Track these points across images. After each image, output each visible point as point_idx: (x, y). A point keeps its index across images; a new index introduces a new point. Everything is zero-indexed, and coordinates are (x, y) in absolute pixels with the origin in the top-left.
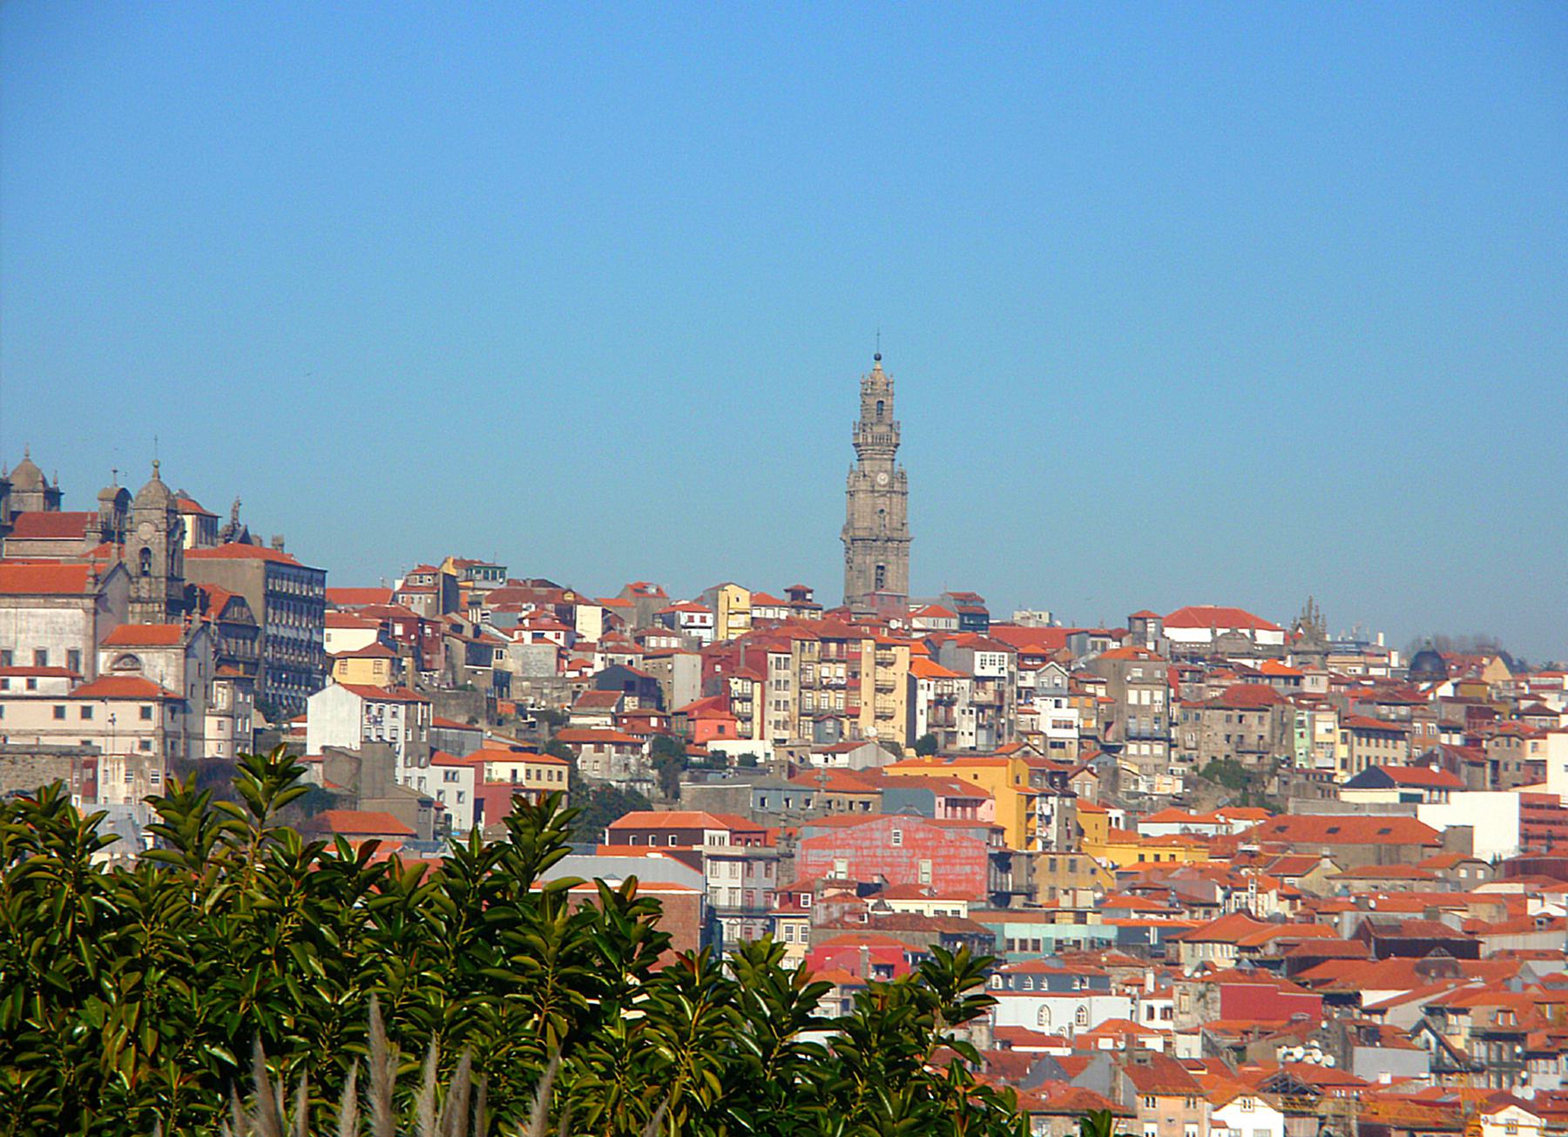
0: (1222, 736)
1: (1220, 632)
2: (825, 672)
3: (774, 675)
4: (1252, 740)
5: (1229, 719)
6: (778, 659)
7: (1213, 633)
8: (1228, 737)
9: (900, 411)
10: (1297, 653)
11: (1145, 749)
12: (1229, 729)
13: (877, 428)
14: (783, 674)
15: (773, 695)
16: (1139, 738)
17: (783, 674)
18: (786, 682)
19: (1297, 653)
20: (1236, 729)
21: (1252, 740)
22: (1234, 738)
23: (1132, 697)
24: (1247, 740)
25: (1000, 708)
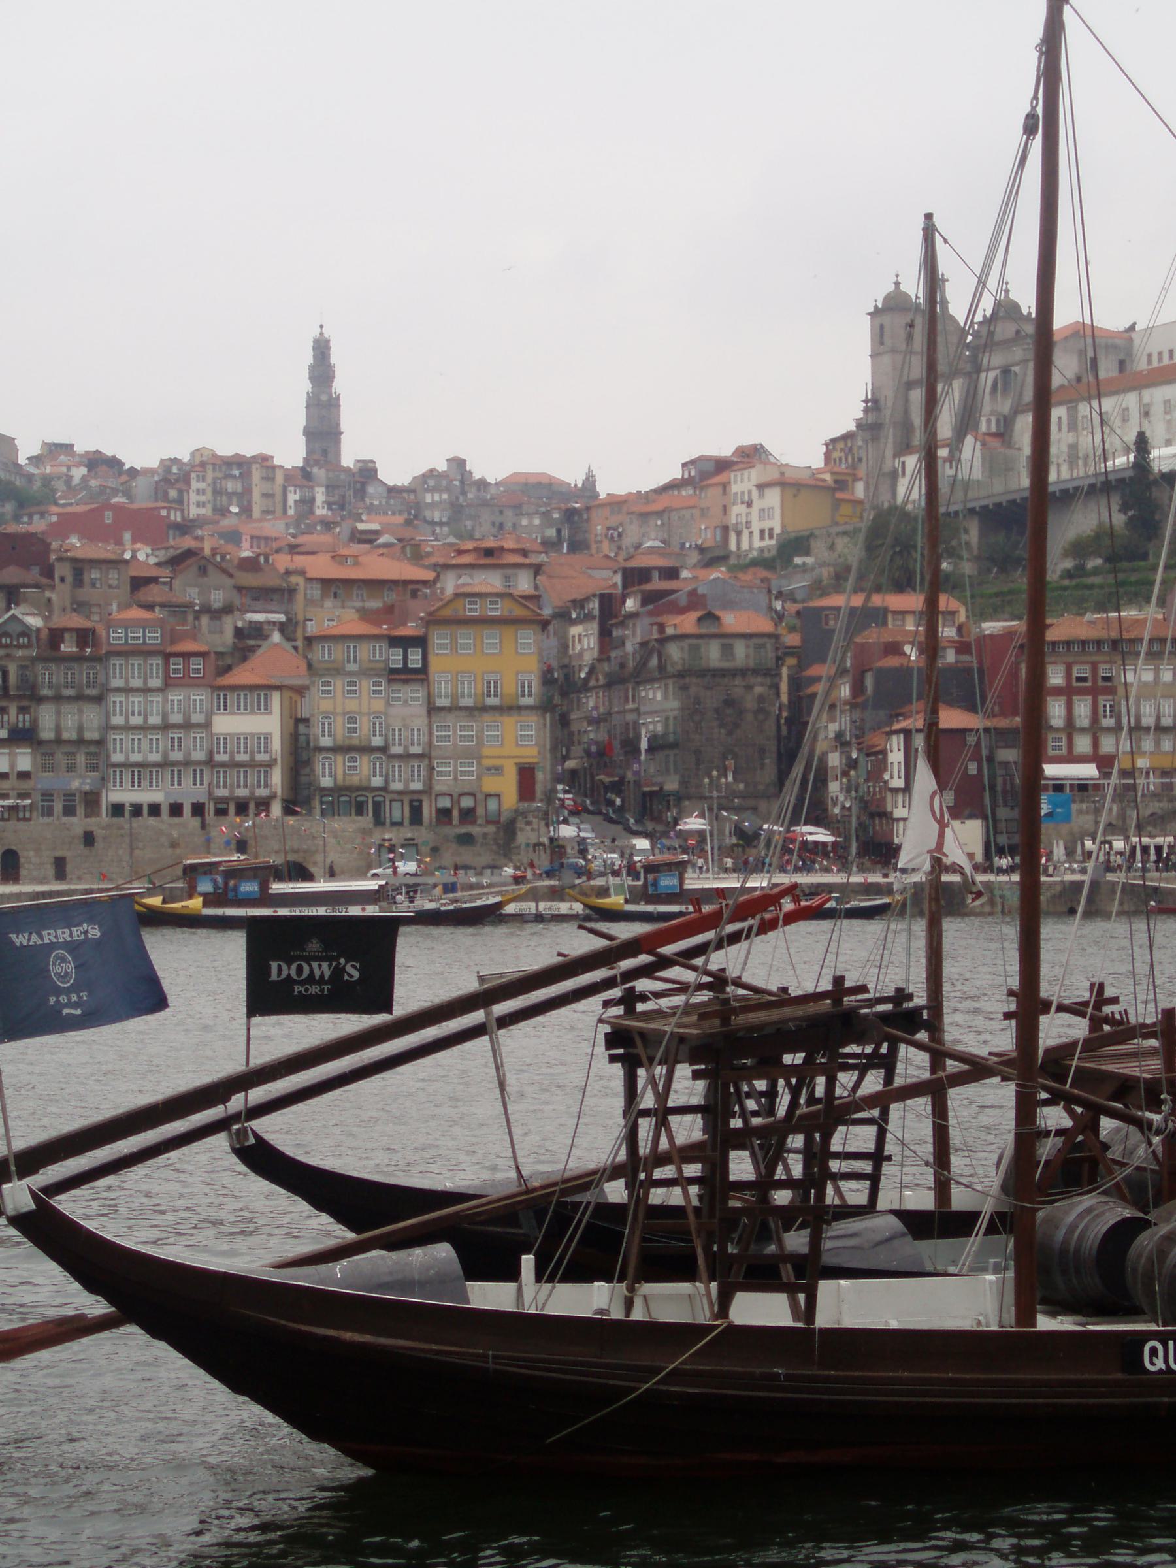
3: (195, 485)
8: (493, 524)
9: (335, 358)
13: (322, 370)
14: (202, 485)
15: (194, 498)
17: (202, 485)
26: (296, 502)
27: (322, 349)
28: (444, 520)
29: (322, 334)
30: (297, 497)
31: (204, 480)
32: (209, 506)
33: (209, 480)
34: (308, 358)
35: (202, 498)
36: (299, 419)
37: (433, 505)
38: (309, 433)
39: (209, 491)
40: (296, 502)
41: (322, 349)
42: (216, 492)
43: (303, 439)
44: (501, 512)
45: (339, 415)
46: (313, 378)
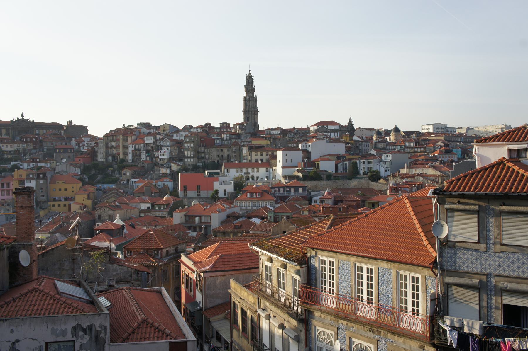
0: (216, 155)
2: (113, 144)
4: (225, 156)
5: (218, 151)
8: (218, 156)
11: (189, 160)
12: (218, 153)
16: (187, 157)
22: (220, 156)
23: (185, 145)
24: (224, 156)
26: (132, 151)
27: (250, 80)
28: (192, 156)
29: (250, 74)
30: (133, 149)
32: (104, 154)
34: (245, 83)
37: (187, 149)
38: (246, 112)
40: (132, 151)
41: (250, 80)
43: (243, 113)
44: (222, 150)
46: (247, 90)
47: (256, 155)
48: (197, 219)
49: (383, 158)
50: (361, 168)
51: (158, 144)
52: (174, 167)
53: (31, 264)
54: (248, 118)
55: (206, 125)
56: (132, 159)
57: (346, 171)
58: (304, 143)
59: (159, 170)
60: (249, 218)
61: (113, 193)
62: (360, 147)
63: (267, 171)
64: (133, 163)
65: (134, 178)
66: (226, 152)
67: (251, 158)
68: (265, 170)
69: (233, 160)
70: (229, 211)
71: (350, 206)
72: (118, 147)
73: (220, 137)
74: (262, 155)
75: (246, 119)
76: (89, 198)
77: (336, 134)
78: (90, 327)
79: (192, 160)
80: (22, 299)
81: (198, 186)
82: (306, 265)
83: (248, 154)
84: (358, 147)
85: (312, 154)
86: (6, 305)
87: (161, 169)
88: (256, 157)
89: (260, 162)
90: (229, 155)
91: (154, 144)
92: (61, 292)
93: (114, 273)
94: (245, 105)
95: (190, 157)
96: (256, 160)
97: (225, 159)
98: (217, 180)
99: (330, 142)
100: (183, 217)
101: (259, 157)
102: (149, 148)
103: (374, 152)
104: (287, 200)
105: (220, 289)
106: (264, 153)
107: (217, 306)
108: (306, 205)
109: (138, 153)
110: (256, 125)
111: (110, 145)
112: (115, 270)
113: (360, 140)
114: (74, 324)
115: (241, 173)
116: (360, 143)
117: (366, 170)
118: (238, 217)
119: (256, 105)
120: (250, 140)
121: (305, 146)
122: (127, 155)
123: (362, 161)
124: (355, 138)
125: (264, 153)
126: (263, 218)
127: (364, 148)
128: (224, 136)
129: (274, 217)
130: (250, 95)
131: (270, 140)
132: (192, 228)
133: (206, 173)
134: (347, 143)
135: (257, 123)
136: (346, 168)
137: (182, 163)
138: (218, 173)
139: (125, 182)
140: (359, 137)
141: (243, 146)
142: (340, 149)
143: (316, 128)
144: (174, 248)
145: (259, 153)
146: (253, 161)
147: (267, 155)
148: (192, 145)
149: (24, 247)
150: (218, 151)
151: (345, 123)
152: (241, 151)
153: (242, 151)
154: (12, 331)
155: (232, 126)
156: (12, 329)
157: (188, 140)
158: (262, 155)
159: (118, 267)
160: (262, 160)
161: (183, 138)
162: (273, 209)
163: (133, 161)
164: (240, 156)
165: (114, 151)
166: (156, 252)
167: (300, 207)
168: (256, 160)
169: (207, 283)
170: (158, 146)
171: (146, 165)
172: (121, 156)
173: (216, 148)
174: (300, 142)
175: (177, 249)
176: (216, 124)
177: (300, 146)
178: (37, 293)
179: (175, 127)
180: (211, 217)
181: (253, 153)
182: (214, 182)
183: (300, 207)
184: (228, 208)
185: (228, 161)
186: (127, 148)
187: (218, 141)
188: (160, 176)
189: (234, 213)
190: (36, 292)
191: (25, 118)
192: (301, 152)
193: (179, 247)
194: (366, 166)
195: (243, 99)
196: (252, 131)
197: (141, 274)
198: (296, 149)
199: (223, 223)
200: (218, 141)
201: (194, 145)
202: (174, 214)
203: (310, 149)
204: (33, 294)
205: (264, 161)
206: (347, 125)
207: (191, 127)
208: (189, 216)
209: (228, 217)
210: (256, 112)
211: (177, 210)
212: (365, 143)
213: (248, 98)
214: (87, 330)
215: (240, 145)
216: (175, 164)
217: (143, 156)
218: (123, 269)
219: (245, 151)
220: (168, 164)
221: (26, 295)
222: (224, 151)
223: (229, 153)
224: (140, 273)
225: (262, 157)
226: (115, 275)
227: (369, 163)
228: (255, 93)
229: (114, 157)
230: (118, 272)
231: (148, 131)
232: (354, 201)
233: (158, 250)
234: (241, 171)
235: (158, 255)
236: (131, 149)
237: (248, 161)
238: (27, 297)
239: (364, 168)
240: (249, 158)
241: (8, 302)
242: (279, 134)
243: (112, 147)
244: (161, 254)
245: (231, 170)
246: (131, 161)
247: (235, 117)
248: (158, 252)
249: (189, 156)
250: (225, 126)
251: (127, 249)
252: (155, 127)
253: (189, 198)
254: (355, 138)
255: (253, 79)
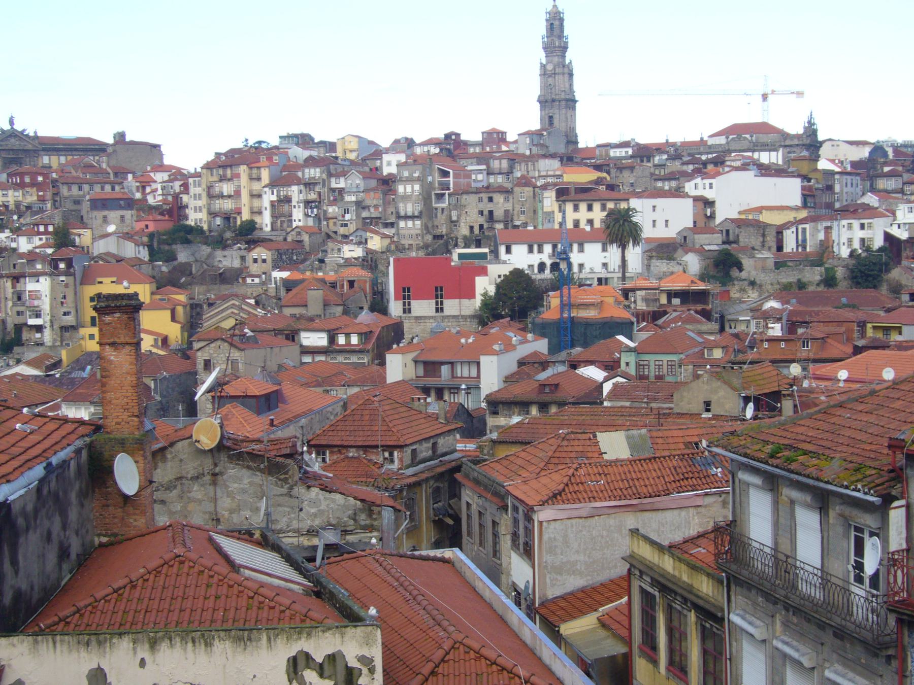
0: (476, 211)
1: (731, 137)
5: (480, 200)
6: (195, 181)
7: (727, 138)
10: (785, 146)
11: (410, 224)
12: (481, 206)
14: (198, 190)
16: (406, 217)
17: (198, 190)
18: (200, 195)
19: (785, 146)
20: (487, 207)
21: (499, 213)
24: (495, 214)
25: (320, 202)
26: (272, 203)
29: (555, 6)
31: (200, 185)
32: (205, 211)
33: (204, 186)
34: (542, 29)
35: (199, 203)
36: (534, 88)
37: (406, 198)
38: (545, 102)
39: (204, 195)
42: (211, 196)
43: (538, 105)
44: (491, 199)
45: (541, 82)
46: (549, 49)
47: (576, 208)
48: (445, 370)
49: (899, 214)
50: (844, 239)
51: (334, 185)
52: (375, 243)
53: (141, 489)
54: (551, 118)
55: (448, 136)
56: (272, 224)
57: (804, 247)
58: (698, 180)
59: (339, 250)
60: (574, 366)
61: (233, 306)
62: (837, 188)
63: (604, 250)
64: (274, 233)
65: (277, 266)
66: (500, 204)
67: (564, 218)
68: (599, 246)
69: (517, 223)
70: (524, 351)
71: (829, 335)
72: (238, 193)
73: (484, 167)
74: (590, 208)
75: (549, 121)
76: (173, 319)
77: (773, 154)
78: (332, 658)
79: (418, 223)
80: (150, 582)
81: (436, 288)
82: (903, 502)
83: (556, 209)
84: (830, 188)
85: (717, 205)
86: (115, 595)
87: (346, 248)
88: (576, 216)
89: (588, 228)
90: (506, 212)
91: (324, 185)
92: (241, 566)
93: (313, 511)
94: (545, 86)
95: (413, 217)
96: (577, 223)
97: (499, 221)
98: (483, 272)
99: (763, 175)
100: (411, 365)
101: (583, 214)
102: (313, 196)
103: (871, 199)
104: (660, 322)
105: (577, 552)
106: (597, 206)
107: (572, 594)
108: (711, 333)
109: (286, 208)
110: (571, 139)
111: (217, 189)
112: (314, 503)
113: (837, 169)
114: (293, 649)
115: (541, 256)
116: (837, 177)
117: (856, 245)
118: (544, 365)
119: (571, 85)
120: (558, 173)
121: (700, 186)
122: (260, 213)
123: (844, 222)
124: (823, 164)
125: (597, 206)
126: (611, 367)
127: (845, 190)
128: (495, 164)
129: (638, 366)
130: (556, 59)
131: (608, 173)
132: (433, 394)
133: (455, 257)
134: (805, 178)
135: (573, 129)
136: (804, 241)
137: (393, 231)
138: (483, 256)
139: (257, 280)
140: (833, 161)
141: (544, 187)
142: (789, 191)
143: (722, 140)
144: (430, 445)
145: (583, 206)
146: (570, 225)
147: (603, 208)
148: (417, 187)
149: (123, 445)
150: (480, 200)
151: (795, 127)
152: (536, 198)
153: (541, 201)
154: (143, 663)
155: (511, 137)
156: (143, 660)
157: (406, 174)
158: (590, 208)
159: (322, 495)
160: (590, 222)
161: (393, 170)
162: (632, 344)
163: (273, 229)
164: (535, 212)
165: (227, 205)
166: (387, 454)
167: (700, 340)
168: (577, 223)
169: (545, 537)
170: (333, 190)
171: (306, 238)
172: (246, 216)
173: (476, 193)
174: (690, 176)
175: (434, 445)
176: (472, 134)
177: (689, 187)
178: (185, 569)
179: (371, 143)
180: (478, 364)
181: (569, 207)
182: (477, 279)
183: (700, 340)
184: (521, 343)
185: (506, 227)
186: (260, 196)
187: (480, 177)
188: (340, 266)
189: (536, 354)
190: (182, 563)
191: (18, 127)
192: (690, 201)
193: (441, 441)
194: (859, 234)
195: (537, 71)
196: (561, 149)
197: (379, 513)
198: (678, 193)
199: (508, 379)
200: (480, 177)
201: (422, 186)
202: (389, 358)
203: (709, 194)
204: (175, 569)
205: (597, 224)
206: (801, 131)
207: (410, 143)
208: (426, 363)
209: (521, 363)
210: (571, 103)
211: (395, 346)
212: (849, 178)
213: (550, 67)
214: (326, 666)
215: (535, 187)
216: (377, 233)
217: (298, 215)
218: (334, 501)
219: (549, 201)
220: (359, 233)
221: (157, 571)
222: (495, 200)
223: (509, 206)
224: (374, 508)
225: (590, 215)
226: (315, 515)
227: (862, 227)
228: (569, 56)
229: (228, 218)
230: (322, 508)
231: (306, 154)
232: (840, 323)
233: (391, 448)
234: (540, 251)
235: (392, 461)
236: (269, 197)
237: (557, 226)
238: (163, 576)
239: (850, 240)
240: (558, 217)
241: (120, 588)
242: (632, 157)
243: (221, 196)
244: (401, 460)
245: (514, 248)
246: (268, 229)
247: (521, 117)
248: (391, 454)
249: (409, 214)
250: (495, 137)
251: (315, 446)
252: (323, 143)
253: (417, 318)
254: (823, 164)
255: (562, 20)
